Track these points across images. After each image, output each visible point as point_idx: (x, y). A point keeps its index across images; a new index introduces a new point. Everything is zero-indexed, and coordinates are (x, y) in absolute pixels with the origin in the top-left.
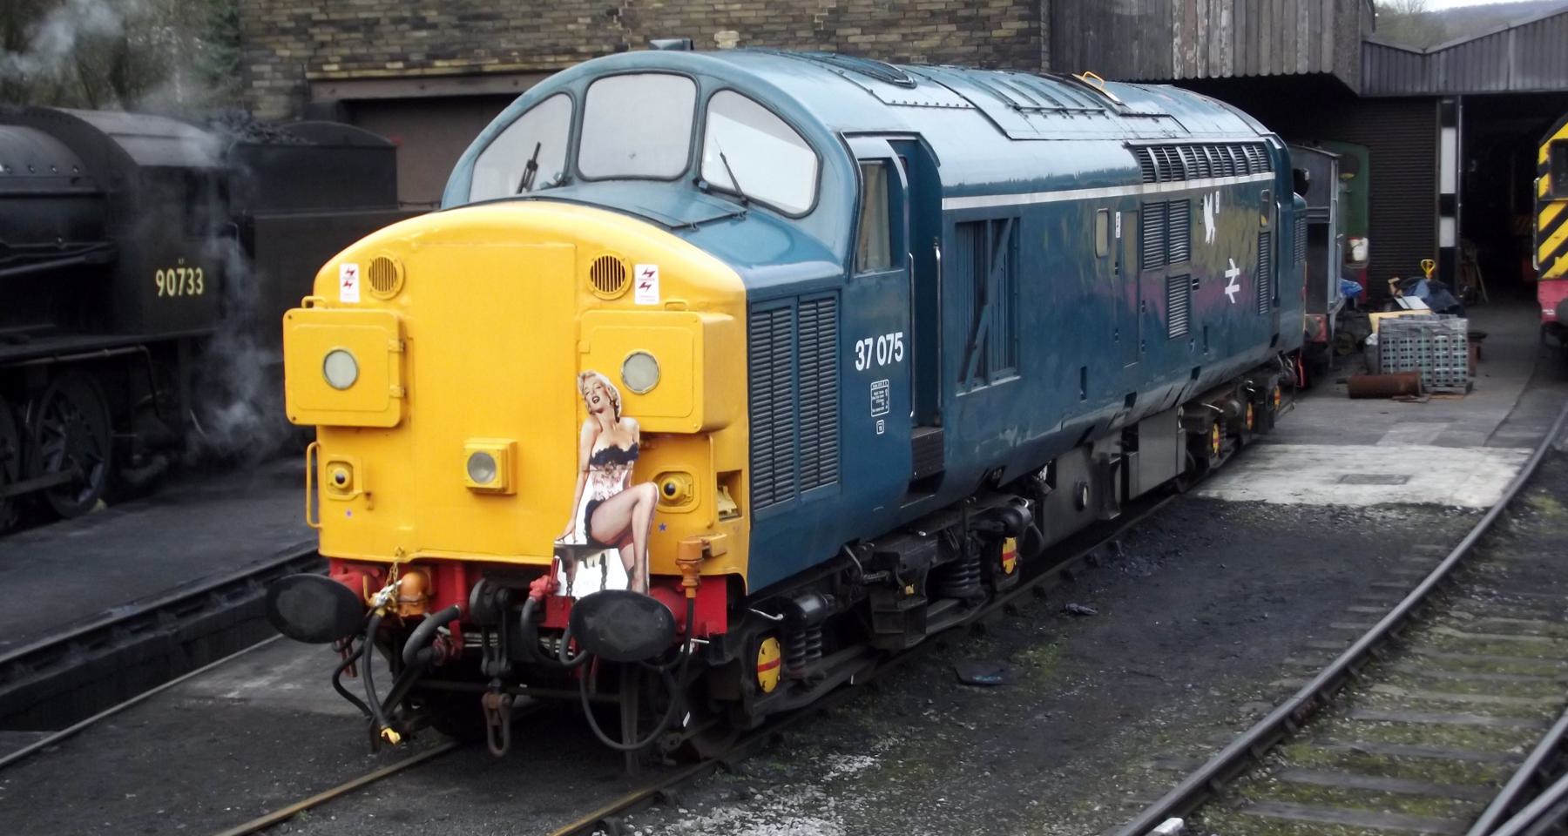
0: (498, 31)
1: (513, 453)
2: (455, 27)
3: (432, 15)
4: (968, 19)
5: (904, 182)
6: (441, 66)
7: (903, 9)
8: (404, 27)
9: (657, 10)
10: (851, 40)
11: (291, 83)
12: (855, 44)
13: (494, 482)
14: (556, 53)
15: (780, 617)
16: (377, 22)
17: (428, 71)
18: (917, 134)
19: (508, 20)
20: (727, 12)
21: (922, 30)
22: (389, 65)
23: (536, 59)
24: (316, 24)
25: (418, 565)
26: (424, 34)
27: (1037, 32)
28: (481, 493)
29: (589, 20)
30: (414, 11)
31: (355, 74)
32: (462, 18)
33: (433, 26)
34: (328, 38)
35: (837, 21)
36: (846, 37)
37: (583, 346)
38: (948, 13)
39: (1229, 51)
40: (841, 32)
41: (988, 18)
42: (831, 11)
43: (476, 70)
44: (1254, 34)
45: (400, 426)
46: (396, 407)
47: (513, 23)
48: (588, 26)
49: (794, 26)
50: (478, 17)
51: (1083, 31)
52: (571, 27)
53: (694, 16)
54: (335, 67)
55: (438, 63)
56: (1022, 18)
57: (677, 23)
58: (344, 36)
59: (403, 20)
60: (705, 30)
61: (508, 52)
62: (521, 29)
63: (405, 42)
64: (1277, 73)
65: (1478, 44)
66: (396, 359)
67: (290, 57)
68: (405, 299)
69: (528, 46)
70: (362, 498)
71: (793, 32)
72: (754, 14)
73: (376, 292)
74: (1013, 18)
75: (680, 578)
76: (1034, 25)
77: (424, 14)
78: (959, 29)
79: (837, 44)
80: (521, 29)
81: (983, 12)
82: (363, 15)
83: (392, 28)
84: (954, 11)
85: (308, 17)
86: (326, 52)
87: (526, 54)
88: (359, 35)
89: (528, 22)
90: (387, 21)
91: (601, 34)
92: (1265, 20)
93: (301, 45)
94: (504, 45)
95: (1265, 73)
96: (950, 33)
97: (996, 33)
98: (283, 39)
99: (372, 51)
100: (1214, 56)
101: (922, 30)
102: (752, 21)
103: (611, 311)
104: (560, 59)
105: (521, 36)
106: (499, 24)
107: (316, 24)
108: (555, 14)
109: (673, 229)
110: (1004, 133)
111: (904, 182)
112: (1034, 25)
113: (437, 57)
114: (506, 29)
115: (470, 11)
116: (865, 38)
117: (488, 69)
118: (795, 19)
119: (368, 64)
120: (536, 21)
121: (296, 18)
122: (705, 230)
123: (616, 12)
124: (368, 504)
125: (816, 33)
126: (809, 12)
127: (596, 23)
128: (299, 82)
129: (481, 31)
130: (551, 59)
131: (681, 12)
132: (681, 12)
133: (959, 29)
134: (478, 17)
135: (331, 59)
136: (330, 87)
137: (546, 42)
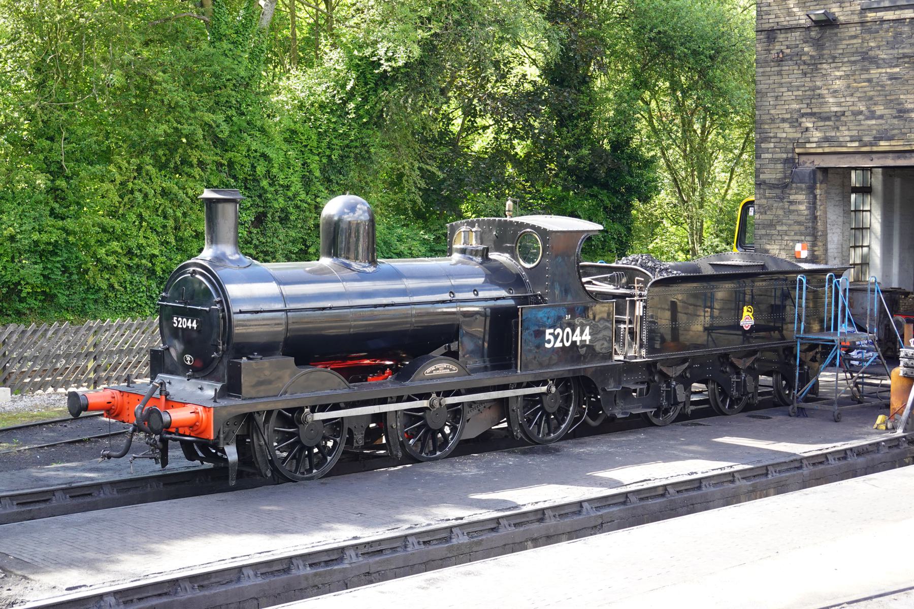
2: (895, 118)
3: (880, 110)
6: (884, 145)
8: (861, 117)
11: (784, 156)
17: (875, 149)
22: (849, 145)
26: (873, 122)
31: (827, 150)
32: (900, 111)
33: (881, 117)
54: (814, 145)
55: (882, 143)
59: (861, 113)
67: (786, 138)
83: (852, 118)
99: (838, 134)
107: (803, 115)
113: (881, 139)
119: (836, 144)
128: (790, 155)
136: (812, 158)
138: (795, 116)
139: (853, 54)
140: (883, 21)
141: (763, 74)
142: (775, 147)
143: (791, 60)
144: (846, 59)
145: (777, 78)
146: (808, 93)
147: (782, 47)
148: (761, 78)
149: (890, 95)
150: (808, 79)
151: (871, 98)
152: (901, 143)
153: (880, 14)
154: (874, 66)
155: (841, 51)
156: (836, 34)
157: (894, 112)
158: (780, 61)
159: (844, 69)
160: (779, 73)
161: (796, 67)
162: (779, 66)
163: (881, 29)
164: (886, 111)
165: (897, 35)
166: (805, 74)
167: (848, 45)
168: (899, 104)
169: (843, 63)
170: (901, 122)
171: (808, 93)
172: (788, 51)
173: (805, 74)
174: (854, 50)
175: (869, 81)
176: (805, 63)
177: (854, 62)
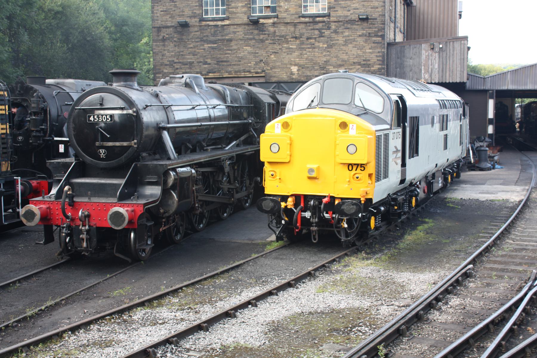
0: (228, 65)
1: (318, 168)
3: (209, 61)
4: (364, 64)
5: (401, 106)
7: (345, 61)
8: (201, 64)
9: (274, 60)
10: (330, 70)
13: (314, 175)
14: (244, 72)
15: (375, 211)
16: (193, 62)
18: (401, 95)
19: (231, 62)
20: (295, 61)
21: (351, 67)
23: (239, 73)
24: (175, 63)
25: (292, 195)
26: (206, 66)
28: (309, 178)
29: (254, 63)
30: (204, 60)
32: (218, 62)
33: (209, 64)
34: (179, 67)
35: (326, 64)
36: (329, 69)
37: (337, 142)
38: (358, 63)
39: (437, 76)
41: (370, 64)
42: (325, 61)
43: (221, 76)
44: (444, 71)
45: (289, 162)
46: (289, 157)
47: (232, 63)
48: (254, 64)
49: (314, 65)
50: (222, 61)
51: (396, 68)
52: (249, 65)
53: (285, 62)
55: (210, 74)
56: (379, 65)
57: (280, 64)
58: (183, 66)
59: (201, 62)
60: (288, 66)
61: (231, 72)
62: (235, 65)
63: (201, 68)
64: (451, 82)
65: (499, 75)
66: (289, 146)
67: (168, 72)
68: (290, 132)
69: (237, 70)
70: (278, 179)
71: (314, 67)
72: (302, 62)
73: (284, 130)
74: (377, 64)
75: (360, 199)
76: (383, 66)
77: (206, 60)
78: (361, 67)
79: (326, 71)
80: (235, 65)
81: (369, 63)
82: (189, 61)
83: (197, 64)
84: (360, 62)
85: (173, 61)
86: (178, 71)
87: (236, 72)
88: (188, 66)
89: (237, 63)
90: (196, 62)
91: (258, 67)
92: (448, 67)
93: (171, 69)
94: (230, 69)
95: (447, 82)
96: (359, 69)
97: (372, 69)
98: (166, 67)
100: (433, 77)
101: (351, 67)
102: (302, 64)
103: (344, 134)
104: (245, 74)
105: (235, 67)
106: (228, 63)
107: (175, 63)
108: (245, 61)
109: (356, 115)
110: (414, 95)
111: (401, 106)
112: (383, 66)
113: (210, 73)
114: (230, 65)
115: (220, 60)
117: (225, 76)
118: (314, 64)
120: (239, 63)
121: (170, 61)
122: (362, 116)
123: (263, 61)
124: (279, 181)
125: (320, 67)
126: (318, 61)
127: (257, 63)
129: (223, 65)
130: (243, 74)
131: (281, 61)
132: (281, 61)
133: (361, 67)
134: (222, 61)
135: (179, 73)
137: (242, 69)
138: (172, 63)
139: (197, 38)
140: (209, 26)
141: (156, 45)
142: (163, 76)
143: (169, 40)
144: (193, 40)
145: (162, 48)
146: (177, 54)
147: (164, 34)
148: (155, 47)
149: (213, 55)
150: (177, 48)
151: (205, 56)
152: (218, 74)
153: (208, 23)
154: (206, 43)
155: (191, 37)
156: (189, 30)
157: (215, 62)
158: (164, 40)
159: (193, 44)
160: (164, 45)
161: (171, 43)
162: (163, 42)
163: (209, 28)
164: (212, 62)
165: (215, 32)
166: (175, 46)
167: (194, 35)
168: (217, 59)
169: (192, 42)
170: (218, 66)
171: (177, 54)
172: (167, 36)
173: (175, 46)
174: (197, 37)
175: (204, 49)
176: (175, 41)
177: (197, 42)
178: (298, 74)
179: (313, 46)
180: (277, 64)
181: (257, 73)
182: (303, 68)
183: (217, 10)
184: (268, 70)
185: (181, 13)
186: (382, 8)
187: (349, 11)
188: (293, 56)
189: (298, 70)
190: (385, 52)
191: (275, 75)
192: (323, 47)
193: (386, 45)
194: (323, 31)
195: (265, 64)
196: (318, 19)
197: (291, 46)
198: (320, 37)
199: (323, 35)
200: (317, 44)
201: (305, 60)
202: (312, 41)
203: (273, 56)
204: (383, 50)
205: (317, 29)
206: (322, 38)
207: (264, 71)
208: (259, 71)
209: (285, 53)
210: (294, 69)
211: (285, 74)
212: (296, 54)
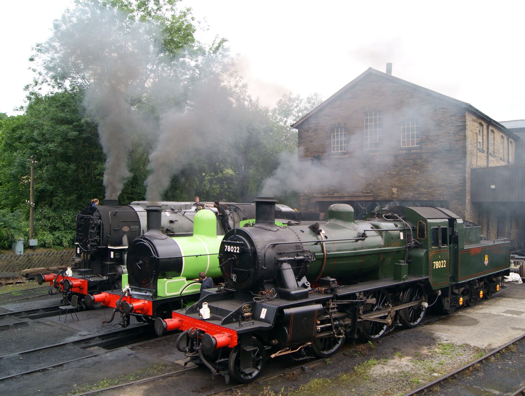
6: (336, 195)
10: (422, 191)
12: (423, 192)
17: (333, 196)
20: (395, 184)
22: (326, 194)
27: (465, 190)
40: (420, 189)
42: (418, 184)
48: (365, 186)
54: (316, 194)
55: (335, 194)
57: (384, 186)
72: (400, 184)
76: (464, 188)
102: (400, 186)
113: (335, 193)
116: (425, 190)
178: (397, 194)
179: (408, 172)
180: (382, 186)
181: (367, 193)
182: (401, 189)
183: (341, 147)
184: (376, 191)
185: (317, 150)
186: (463, 141)
187: (437, 144)
188: (394, 180)
189: (397, 191)
190: (467, 177)
191: (380, 195)
192: (417, 173)
193: (468, 170)
194: (417, 160)
195: (373, 187)
196: (413, 151)
197: (392, 173)
198: (414, 165)
199: (417, 163)
200: (412, 171)
201: (402, 183)
202: (407, 168)
203: (379, 180)
204: (464, 175)
205: (412, 159)
206: (415, 166)
207: (372, 192)
208: (369, 191)
209: (388, 178)
210: (395, 190)
211: (387, 194)
212: (395, 178)
